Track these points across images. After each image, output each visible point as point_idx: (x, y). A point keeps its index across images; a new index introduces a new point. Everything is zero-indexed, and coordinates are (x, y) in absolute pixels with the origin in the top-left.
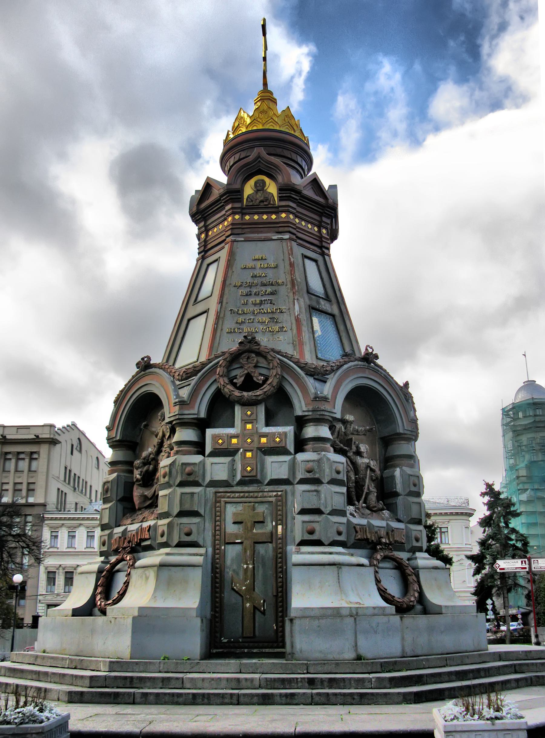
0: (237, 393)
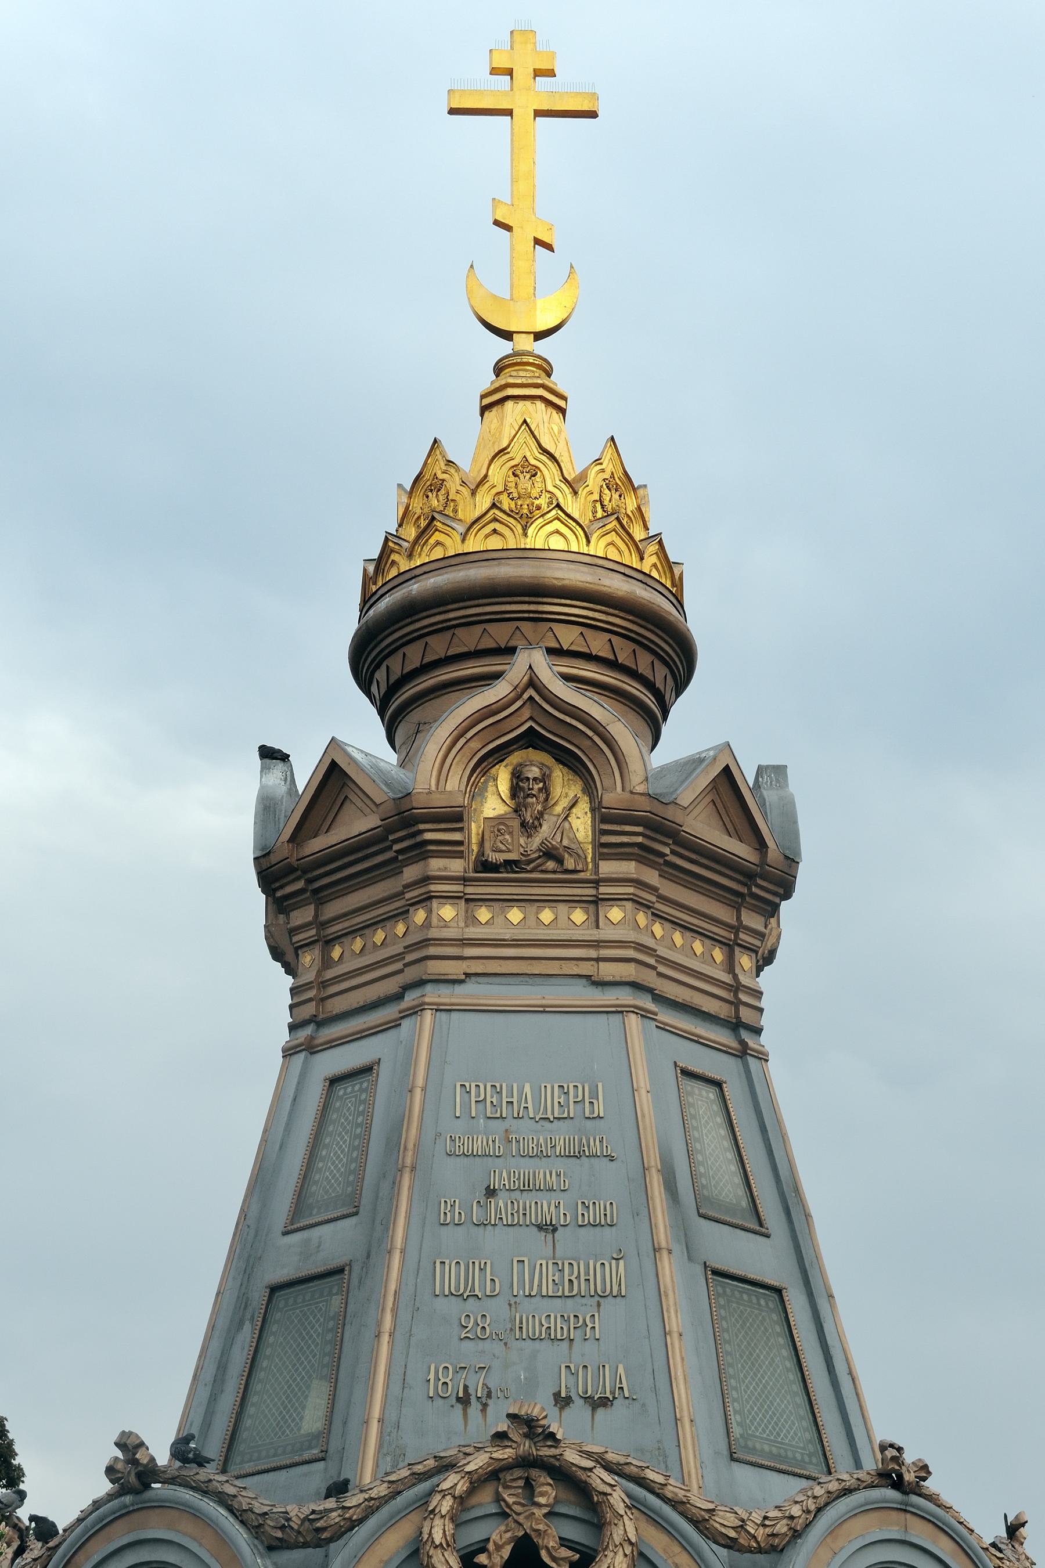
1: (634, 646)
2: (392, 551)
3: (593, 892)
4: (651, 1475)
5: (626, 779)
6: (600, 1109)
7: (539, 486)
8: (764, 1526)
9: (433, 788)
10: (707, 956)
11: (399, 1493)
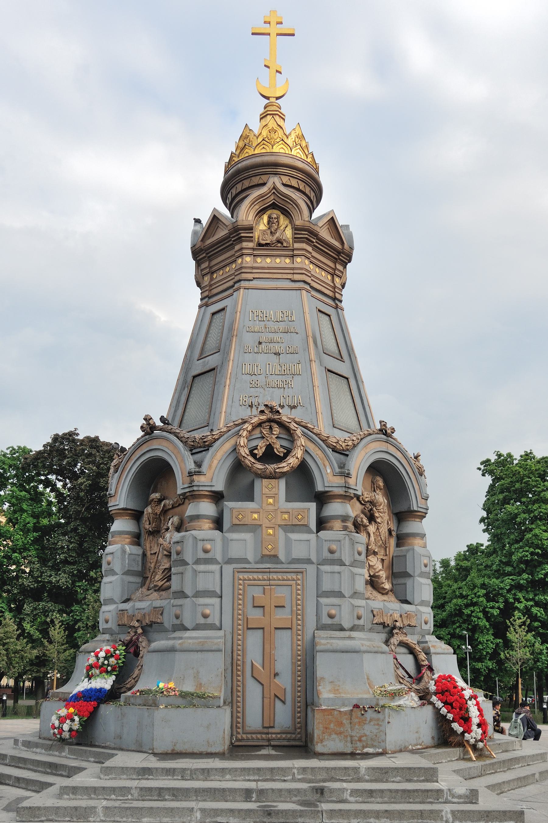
0: (259, 466)
1: (304, 184)
2: (233, 157)
3: (292, 253)
4: (309, 425)
5: (302, 215)
6: (294, 318)
7: (277, 135)
8: (345, 442)
9: (244, 219)
10: (326, 277)
11: (230, 430)
